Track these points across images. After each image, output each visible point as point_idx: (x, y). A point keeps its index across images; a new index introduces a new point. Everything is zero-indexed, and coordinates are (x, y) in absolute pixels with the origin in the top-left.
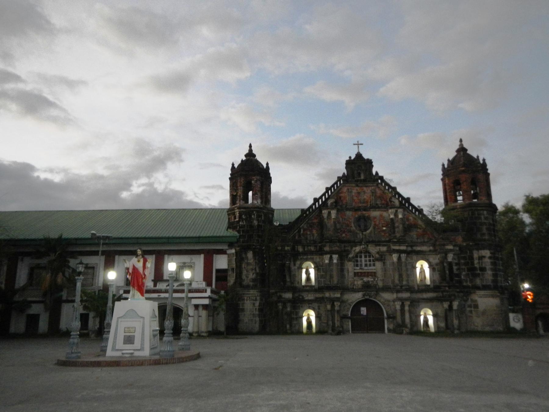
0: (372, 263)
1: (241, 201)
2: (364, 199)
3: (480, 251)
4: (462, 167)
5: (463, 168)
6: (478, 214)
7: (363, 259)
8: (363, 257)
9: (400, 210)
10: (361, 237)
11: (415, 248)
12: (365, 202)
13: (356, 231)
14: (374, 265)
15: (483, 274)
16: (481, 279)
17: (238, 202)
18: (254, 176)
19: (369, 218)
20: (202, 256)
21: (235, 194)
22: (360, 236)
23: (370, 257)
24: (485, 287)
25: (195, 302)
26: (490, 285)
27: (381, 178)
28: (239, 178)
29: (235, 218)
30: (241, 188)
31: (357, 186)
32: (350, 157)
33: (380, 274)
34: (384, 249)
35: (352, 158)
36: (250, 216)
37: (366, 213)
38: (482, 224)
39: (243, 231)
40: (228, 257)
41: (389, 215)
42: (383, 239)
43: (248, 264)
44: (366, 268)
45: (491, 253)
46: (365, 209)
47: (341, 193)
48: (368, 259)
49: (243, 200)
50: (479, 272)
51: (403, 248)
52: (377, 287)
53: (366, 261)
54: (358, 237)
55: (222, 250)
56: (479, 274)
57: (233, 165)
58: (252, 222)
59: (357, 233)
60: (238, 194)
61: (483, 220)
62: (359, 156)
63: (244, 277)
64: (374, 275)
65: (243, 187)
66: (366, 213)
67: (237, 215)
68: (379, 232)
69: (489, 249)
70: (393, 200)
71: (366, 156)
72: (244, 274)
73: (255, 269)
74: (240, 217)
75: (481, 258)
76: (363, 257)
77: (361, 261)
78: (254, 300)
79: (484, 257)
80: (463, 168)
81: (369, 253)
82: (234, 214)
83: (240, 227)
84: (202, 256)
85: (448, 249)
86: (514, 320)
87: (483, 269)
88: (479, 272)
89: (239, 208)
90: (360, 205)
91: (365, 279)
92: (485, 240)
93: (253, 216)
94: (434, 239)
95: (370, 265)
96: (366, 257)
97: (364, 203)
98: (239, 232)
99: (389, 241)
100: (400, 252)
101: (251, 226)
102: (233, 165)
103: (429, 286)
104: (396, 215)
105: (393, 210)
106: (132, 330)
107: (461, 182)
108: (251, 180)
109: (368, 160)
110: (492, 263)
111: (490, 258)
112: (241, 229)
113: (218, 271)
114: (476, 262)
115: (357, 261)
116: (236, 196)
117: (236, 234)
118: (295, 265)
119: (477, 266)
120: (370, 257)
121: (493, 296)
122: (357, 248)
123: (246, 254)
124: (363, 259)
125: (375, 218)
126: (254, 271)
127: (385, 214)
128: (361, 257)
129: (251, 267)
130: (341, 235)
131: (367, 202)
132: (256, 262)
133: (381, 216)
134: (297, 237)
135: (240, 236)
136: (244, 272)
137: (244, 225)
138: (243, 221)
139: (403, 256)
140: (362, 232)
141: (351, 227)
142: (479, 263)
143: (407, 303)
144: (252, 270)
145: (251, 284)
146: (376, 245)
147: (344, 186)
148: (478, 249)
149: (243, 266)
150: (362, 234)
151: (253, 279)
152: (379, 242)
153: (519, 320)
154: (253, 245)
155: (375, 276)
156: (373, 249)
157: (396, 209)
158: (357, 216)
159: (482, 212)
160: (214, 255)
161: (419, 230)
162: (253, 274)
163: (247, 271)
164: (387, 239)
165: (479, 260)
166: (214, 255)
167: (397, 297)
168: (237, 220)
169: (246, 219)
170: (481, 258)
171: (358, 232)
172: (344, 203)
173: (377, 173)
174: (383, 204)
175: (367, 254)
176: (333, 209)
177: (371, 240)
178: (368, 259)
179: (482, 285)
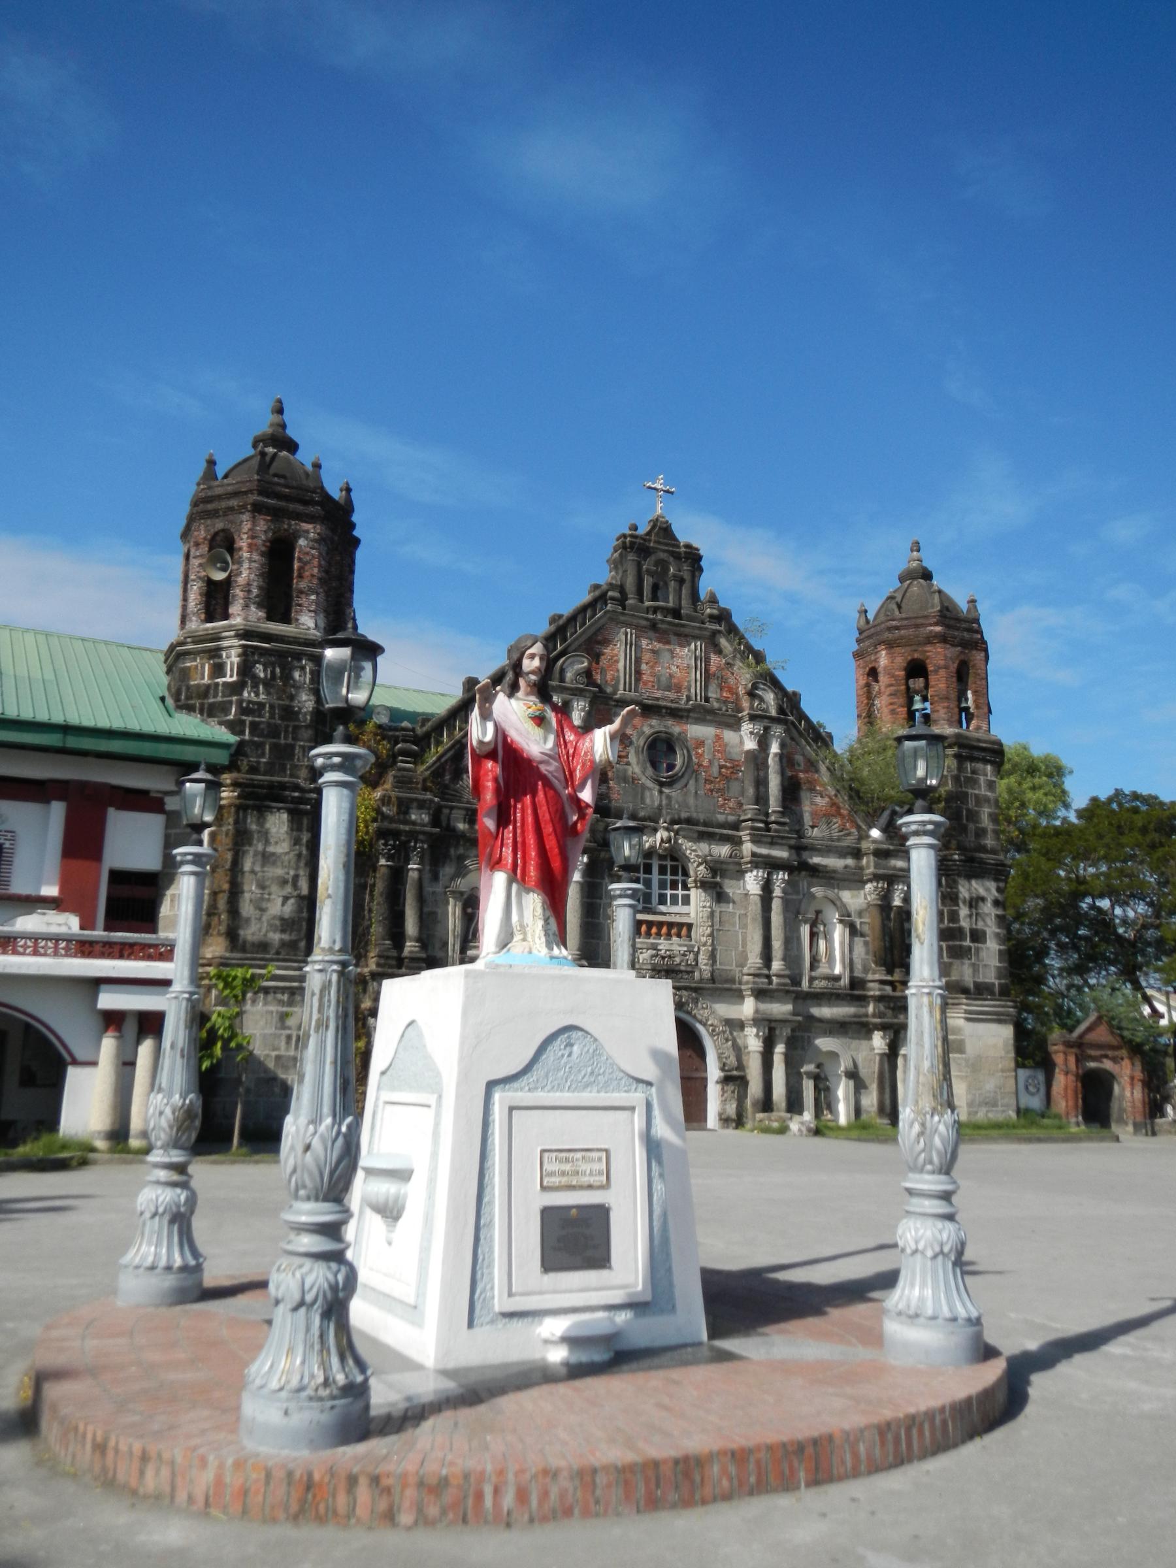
0: (680, 892)
1: (253, 608)
2: (671, 676)
3: (973, 882)
4: (936, 624)
5: (938, 629)
6: (974, 772)
8: (655, 870)
9: (778, 730)
10: (656, 803)
11: (805, 855)
12: (672, 685)
13: (644, 780)
14: (686, 901)
15: (977, 949)
16: (974, 965)
17: (235, 609)
18: (311, 519)
19: (682, 739)
20: (57, 810)
21: (219, 576)
22: (653, 797)
23: (674, 872)
24: (980, 991)
25: (108, 1000)
26: (993, 984)
27: (723, 617)
28: (246, 517)
29: (218, 670)
30: (256, 557)
31: (653, 626)
32: (635, 528)
33: (701, 933)
34: (723, 850)
35: (643, 530)
36: (287, 677)
37: (676, 728)
38: (979, 800)
39: (254, 726)
40: (168, 826)
41: (742, 742)
42: (721, 818)
43: (267, 858)
44: (662, 908)
45: (999, 890)
46: (676, 714)
47: (599, 643)
48: (669, 877)
49: (260, 606)
50: (967, 943)
51: (781, 853)
52: (697, 974)
53: (662, 885)
54: (648, 801)
55: (145, 793)
56: (970, 948)
57: (211, 463)
58: (292, 698)
59: (644, 787)
60: (242, 580)
61: (983, 791)
62: (663, 530)
63: (247, 909)
64: (683, 929)
65: (262, 554)
66: (676, 728)
67: (232, 659)
68: (712, 791)
69: (996, 880)
70: (760, 693)
71: (683, 536)
72: (247, 896)
73: (296, 877)
74: (245, 669)
75: (975, 902)
76: (655, 870)
78: (281, 1003)
79: (983, 899)
80: (938, 629)
82: (215, 653)
83: (244, 711)
84: (57, 810)
85: (895, 868)
86: (1027, 1088)
87: (978, 936)
88: (967, 943)
89: (246, 634)
90: (659, 694)
91: (664, 945)
92: (983, 849)
93: (297, 675)
94: (854, 830)
95: (674, 901)
96: (662, 870)
97: (668, 688)
98: (235, 727)
99: (736, 826)
100: (772, 865)
101: (289, 713)
102: (211, 463)
103: (837, 979)
104: (763, 743)
106: (591, 1169)
107: (930, 668)
108: (295, 536)
109: (688, 546)
110: (1001, 919)
111: (996, 903)
112: (248, 719)
113: (117, 877)
114: (964, 911)
116: (227, 584)
117: (223, 734)
118: (435, 877)
119: (965, 924)
120: (674, 872)
121: (999, 1019)
123: (261, 820)
124: (655, 877)
125: (700, 743)
126: (289, 889)
127: (729, 735)
129: (279, 871)
131: (678, 689)
132: (299, 856)
133: (718, 738)
134: (447, 777)
135: (241, 744)
136: (250, 889)
137: (261, 705)
138: (255, 686)
139: (781, 876)
140: (661, 784)
141: (628, 764)
142: (970, 916)
143: (786, 1032)
144: (284, 882)
145: (276, 937)
146: (703, 836)
147: (611, 619)
148: (969, 877)
149: (247, 865)
150: (661, 792)
151: (282, 919)
152: (705, 824)
153: (1038, 1090)
154: (297, 787)
155: (689, 936)
156: (694, 851)
157: (766, 723)
158: (647, 731)
159: (980, 766)
160: (112, 812)
161: (818, 800)
162: (286, 899)
163: (262, 886)
164: (731, 818)
165: (971, 906)
166: (112, 812)
167: (757, 1011)
168: (231, 677)
169: (267, 684)
170: (975, 902)
171: (649, 784)
172: (609, 677)
173: (713, 600)
174: (725, 702)
175: (669, 863)
176: (578, 693)
177: (684, 815)
178: (669, 877)
179: (975, 983)
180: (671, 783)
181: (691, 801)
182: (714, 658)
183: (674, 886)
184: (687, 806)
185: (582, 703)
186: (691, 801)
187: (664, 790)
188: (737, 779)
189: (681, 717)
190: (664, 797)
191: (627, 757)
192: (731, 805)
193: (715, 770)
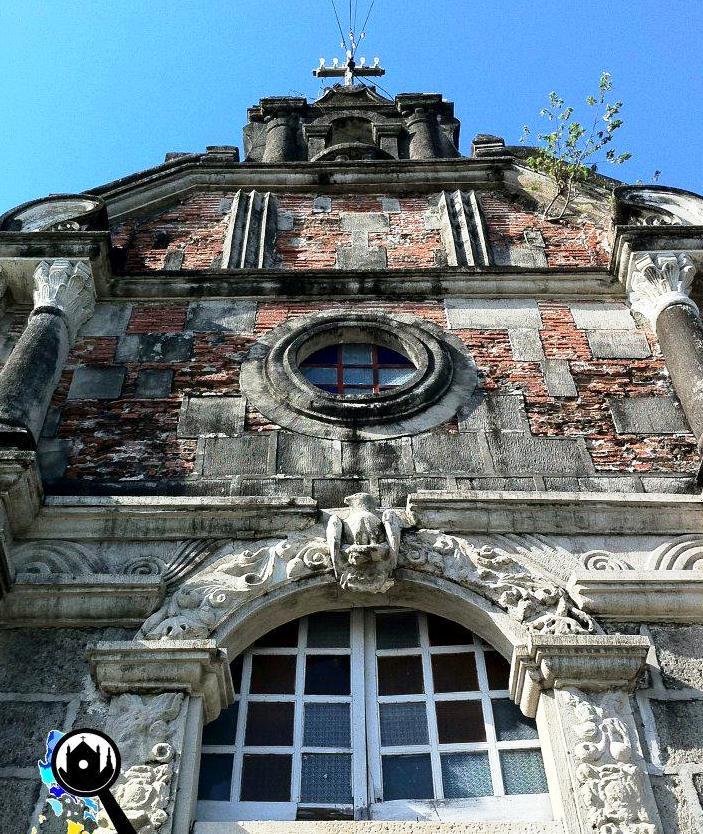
7: (364, 697)
13: (286, 419)
23: (455, 674)
48: (430, 697)
53: (399, 726)
59: (287, 435)
68: (559, 427)
77: (333, 726)
81: (446, 631)
96: (397, 676)
105: (665, 258)
115: (272, 725)
120: (455, 674)
122: (276, 548)
128: (331, 676)
130: (106, 447)
140: (354, 420)
150: (355, 442)
171: (307, 425)
175: (426, 651)
178: (430, 697)
180: (393, 411)
181: (481, 452)
182: (516, 221)
183: (460, 724)
184: (466, 466)
185: (60, 265)
186: (481, 452)
187: (365, 434)
188: (652, 394)
189: (418, 297)
190: (366, 451)
191: (232, 382)
192: (646, 450)
193: (560, 383)
